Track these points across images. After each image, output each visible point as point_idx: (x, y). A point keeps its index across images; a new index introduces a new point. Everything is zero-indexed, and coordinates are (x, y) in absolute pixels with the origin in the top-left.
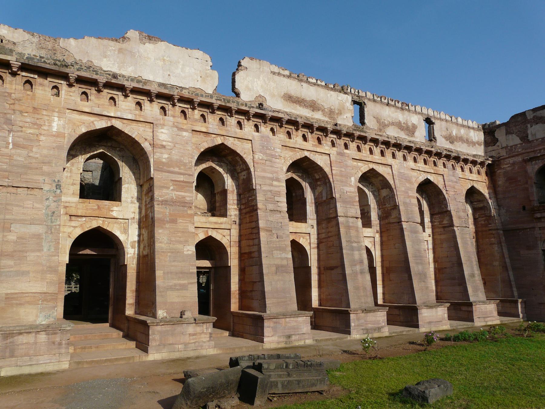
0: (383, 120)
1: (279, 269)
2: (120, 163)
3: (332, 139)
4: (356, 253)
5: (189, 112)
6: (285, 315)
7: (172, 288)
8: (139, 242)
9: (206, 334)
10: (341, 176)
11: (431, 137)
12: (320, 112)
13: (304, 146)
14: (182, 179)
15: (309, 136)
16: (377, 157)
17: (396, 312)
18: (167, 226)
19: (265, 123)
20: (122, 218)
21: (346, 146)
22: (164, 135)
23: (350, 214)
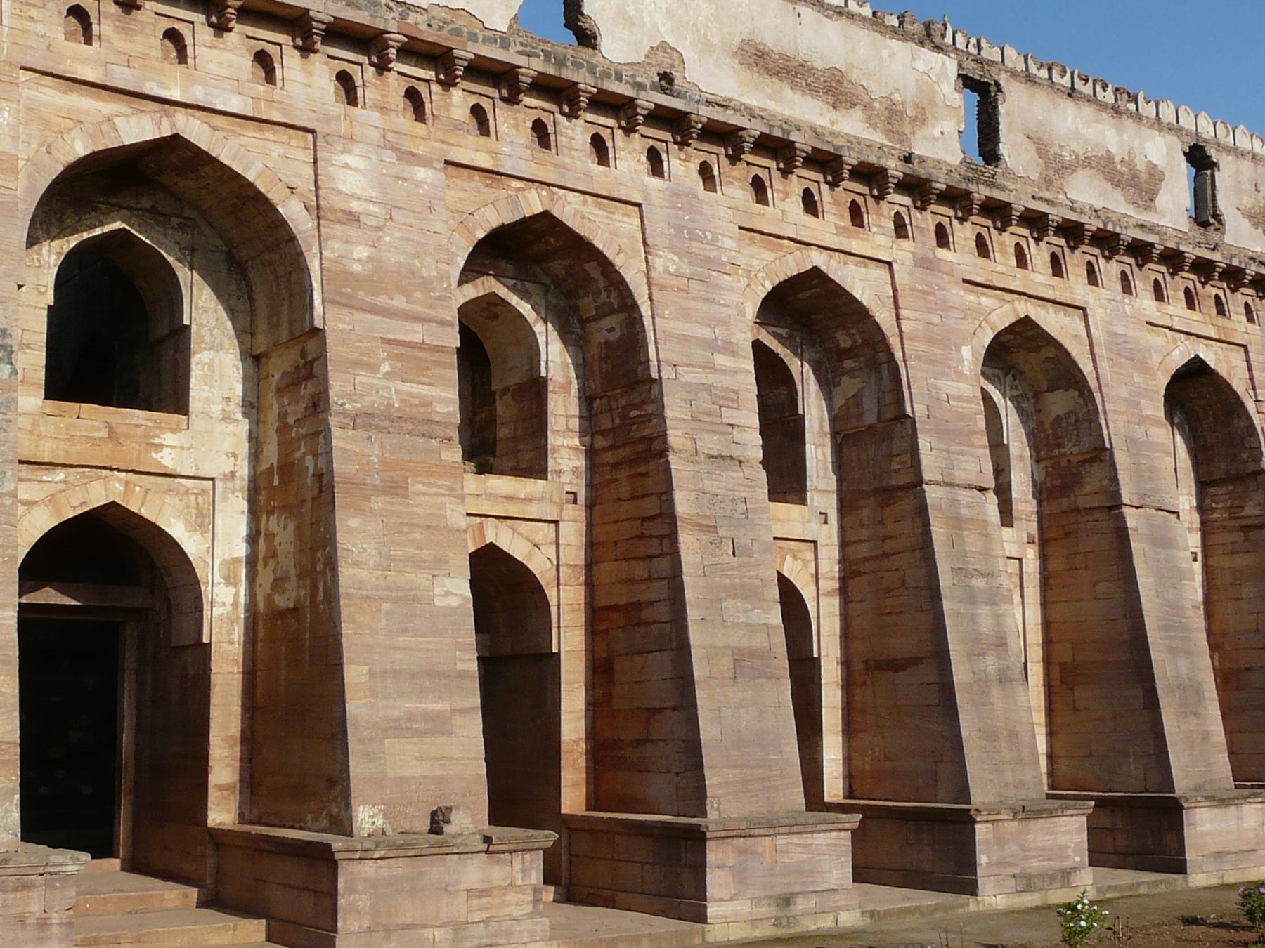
0: (1056, 149)
1: (744, 663)
2: (184, 274)
3: (897, 208)
4: (984, 611)
5: (433, 95)
6: (773, 825)
7: (400, 728)
8: (251, 561)
9: (521, 889)
10: (930, 341)
11: (1205, 213)
12: (858, 113)
14: (418, 338)
15: (825, 195)
16: (1039, 277)
17: (1106, 821)
18: (377, 503)
19: (683, 144)
20: (192, 471)
21: (942, 237)
22: (353, 175)
23: (960, 476)
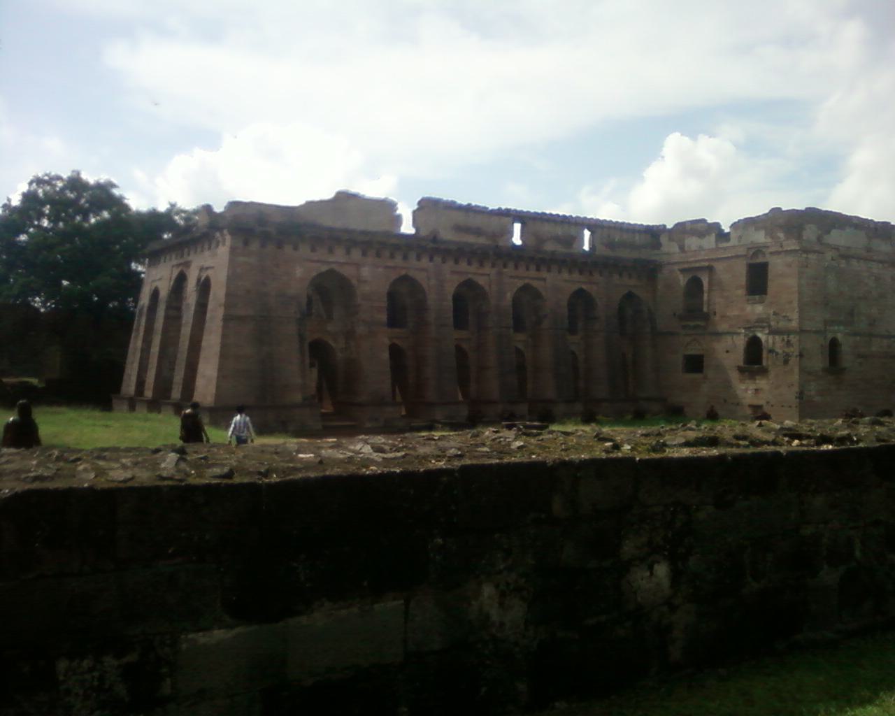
13: (469, 270)
16: (533, 273)
22: (366, 272)
